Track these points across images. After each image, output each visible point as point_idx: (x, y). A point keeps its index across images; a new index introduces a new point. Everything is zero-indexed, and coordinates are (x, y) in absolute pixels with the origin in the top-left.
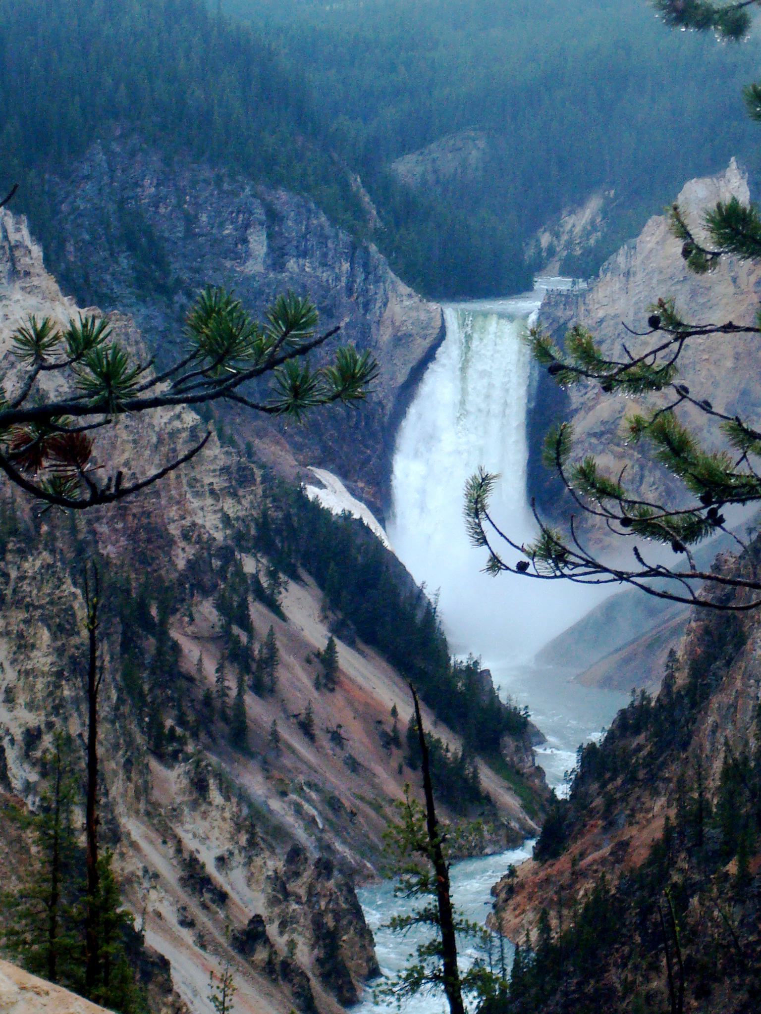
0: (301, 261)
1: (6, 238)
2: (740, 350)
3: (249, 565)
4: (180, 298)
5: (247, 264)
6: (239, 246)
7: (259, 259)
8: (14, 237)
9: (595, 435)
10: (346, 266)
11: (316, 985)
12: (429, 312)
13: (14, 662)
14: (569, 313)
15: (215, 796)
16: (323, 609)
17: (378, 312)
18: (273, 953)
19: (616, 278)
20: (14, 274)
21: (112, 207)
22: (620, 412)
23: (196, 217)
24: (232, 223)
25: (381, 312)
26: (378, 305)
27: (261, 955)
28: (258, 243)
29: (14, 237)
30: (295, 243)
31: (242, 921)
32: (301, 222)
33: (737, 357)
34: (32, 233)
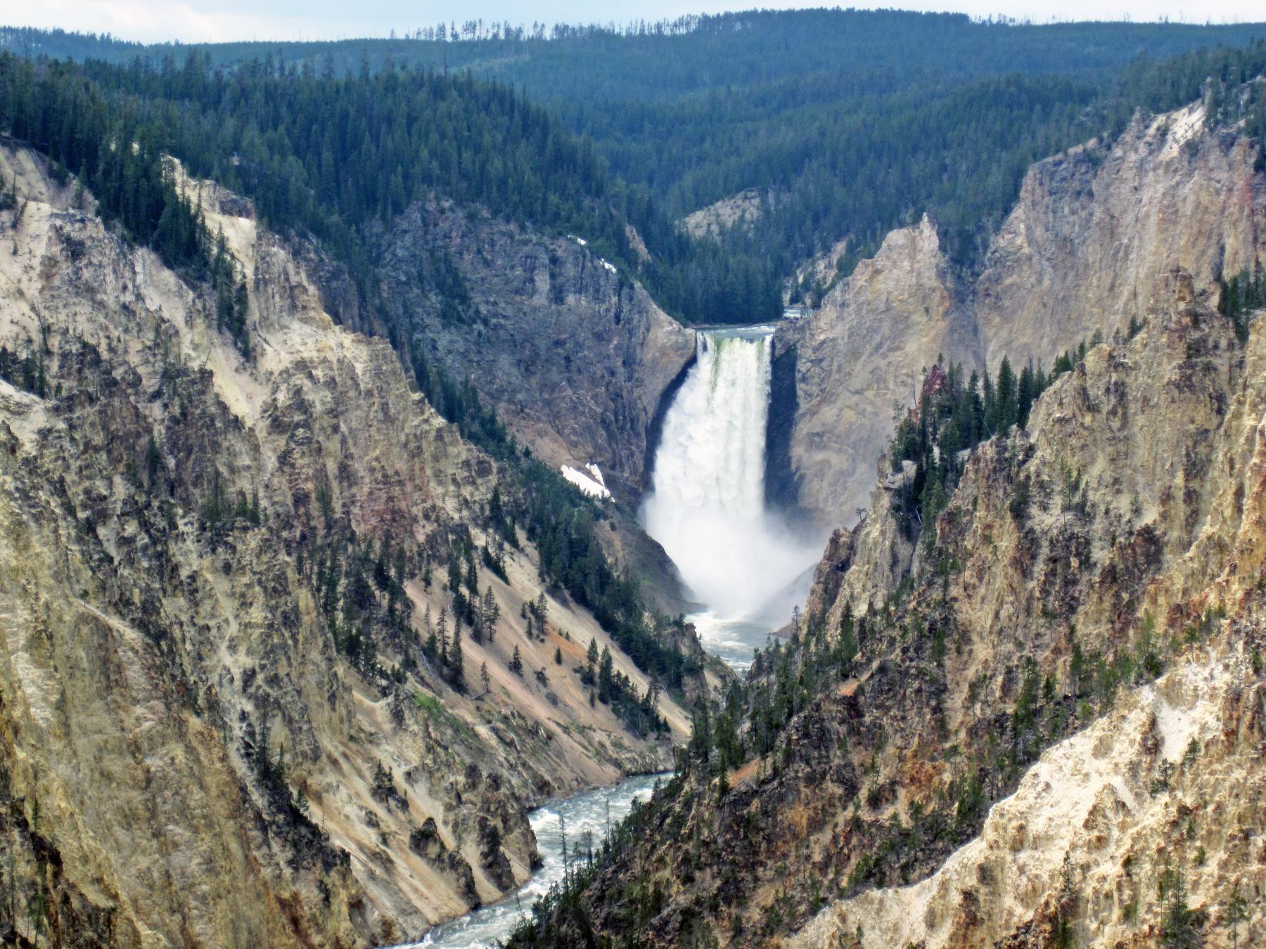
1: (287, 279)
3: (480, 539)
4: (479, 327)
8: (294, 279)
9: (818, 434)
10: (614, 299)
11: (479, 874)
13: (237, 616)
15: (412, 725)
16: (541, 575)
18: (443, 847)
20: (293, 308)
21: (425, 255)
27: (433, 850)
28: (543, 282)
29: (294, 279)
31: (420, 822)
34: (309, 276)
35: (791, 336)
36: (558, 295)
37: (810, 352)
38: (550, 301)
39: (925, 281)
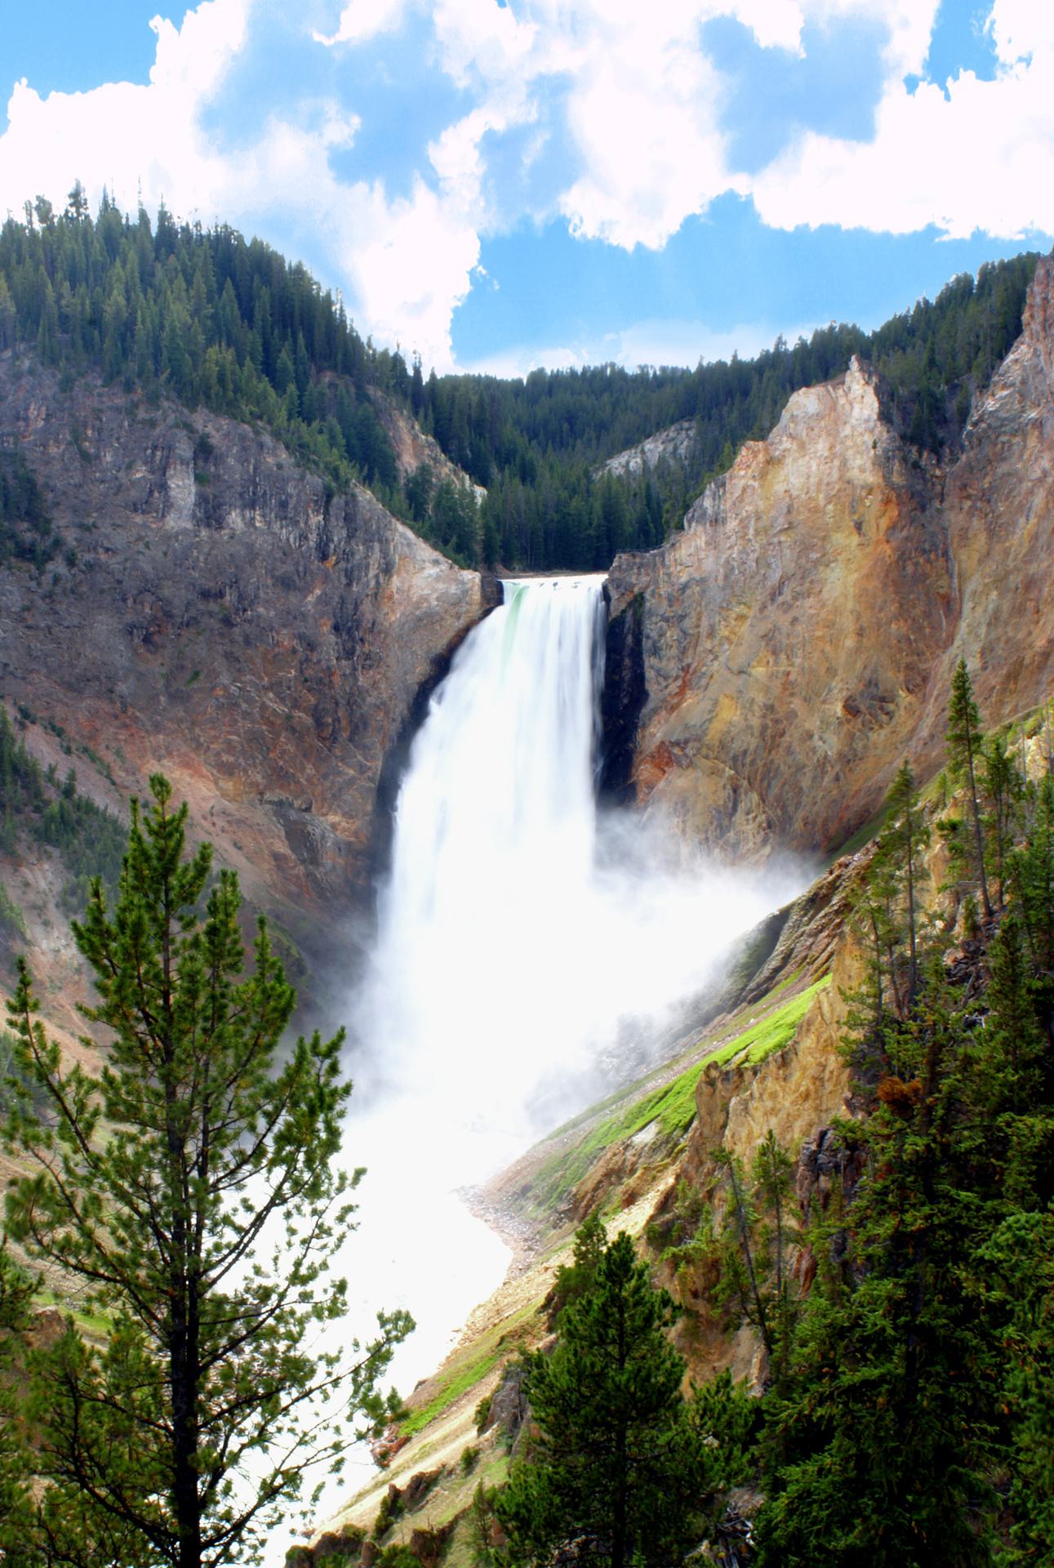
0: (248, 514)
2: (864, 622)
4: (58, 566)
5: (168, 518)
6: (156, 494)
7: (185, 512)
9: (677, 744)
12: (463, 583)
14: (645, 579)
17: (373, 583)
19: (700, 528)
22: (710, 712)
23: (98, 457)
24: (145, 463)
25: (378, 583)
26: (371, 574)
28: (183, 488)
30: (239, 489)
32: (247, 461)
33: (860, 633)
35: (639, 581)
36: (210, 513)
37: (665, 603)
38: (198, 522)
39: (854, 474)
